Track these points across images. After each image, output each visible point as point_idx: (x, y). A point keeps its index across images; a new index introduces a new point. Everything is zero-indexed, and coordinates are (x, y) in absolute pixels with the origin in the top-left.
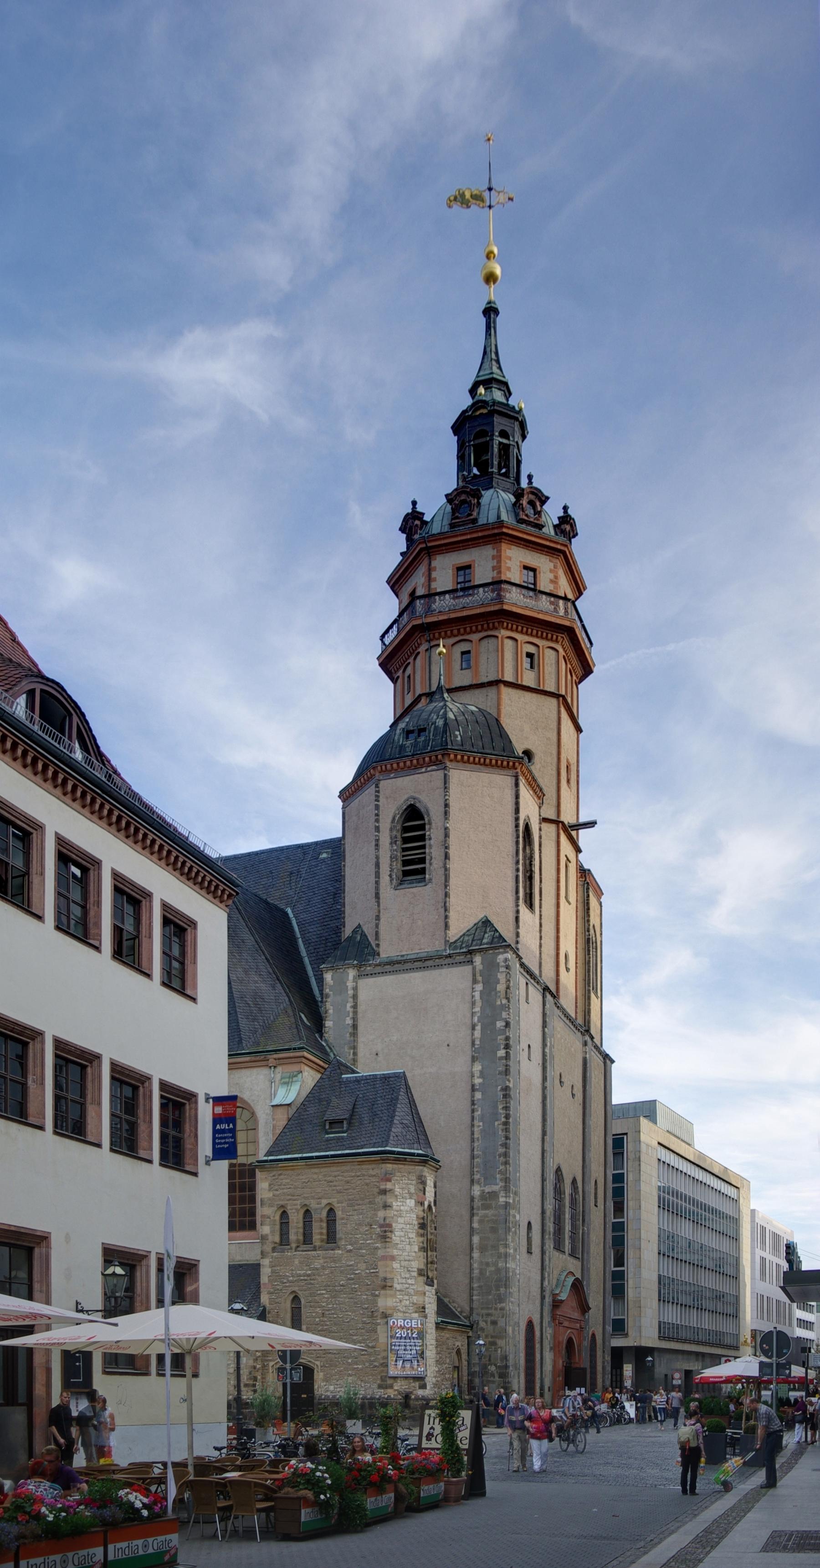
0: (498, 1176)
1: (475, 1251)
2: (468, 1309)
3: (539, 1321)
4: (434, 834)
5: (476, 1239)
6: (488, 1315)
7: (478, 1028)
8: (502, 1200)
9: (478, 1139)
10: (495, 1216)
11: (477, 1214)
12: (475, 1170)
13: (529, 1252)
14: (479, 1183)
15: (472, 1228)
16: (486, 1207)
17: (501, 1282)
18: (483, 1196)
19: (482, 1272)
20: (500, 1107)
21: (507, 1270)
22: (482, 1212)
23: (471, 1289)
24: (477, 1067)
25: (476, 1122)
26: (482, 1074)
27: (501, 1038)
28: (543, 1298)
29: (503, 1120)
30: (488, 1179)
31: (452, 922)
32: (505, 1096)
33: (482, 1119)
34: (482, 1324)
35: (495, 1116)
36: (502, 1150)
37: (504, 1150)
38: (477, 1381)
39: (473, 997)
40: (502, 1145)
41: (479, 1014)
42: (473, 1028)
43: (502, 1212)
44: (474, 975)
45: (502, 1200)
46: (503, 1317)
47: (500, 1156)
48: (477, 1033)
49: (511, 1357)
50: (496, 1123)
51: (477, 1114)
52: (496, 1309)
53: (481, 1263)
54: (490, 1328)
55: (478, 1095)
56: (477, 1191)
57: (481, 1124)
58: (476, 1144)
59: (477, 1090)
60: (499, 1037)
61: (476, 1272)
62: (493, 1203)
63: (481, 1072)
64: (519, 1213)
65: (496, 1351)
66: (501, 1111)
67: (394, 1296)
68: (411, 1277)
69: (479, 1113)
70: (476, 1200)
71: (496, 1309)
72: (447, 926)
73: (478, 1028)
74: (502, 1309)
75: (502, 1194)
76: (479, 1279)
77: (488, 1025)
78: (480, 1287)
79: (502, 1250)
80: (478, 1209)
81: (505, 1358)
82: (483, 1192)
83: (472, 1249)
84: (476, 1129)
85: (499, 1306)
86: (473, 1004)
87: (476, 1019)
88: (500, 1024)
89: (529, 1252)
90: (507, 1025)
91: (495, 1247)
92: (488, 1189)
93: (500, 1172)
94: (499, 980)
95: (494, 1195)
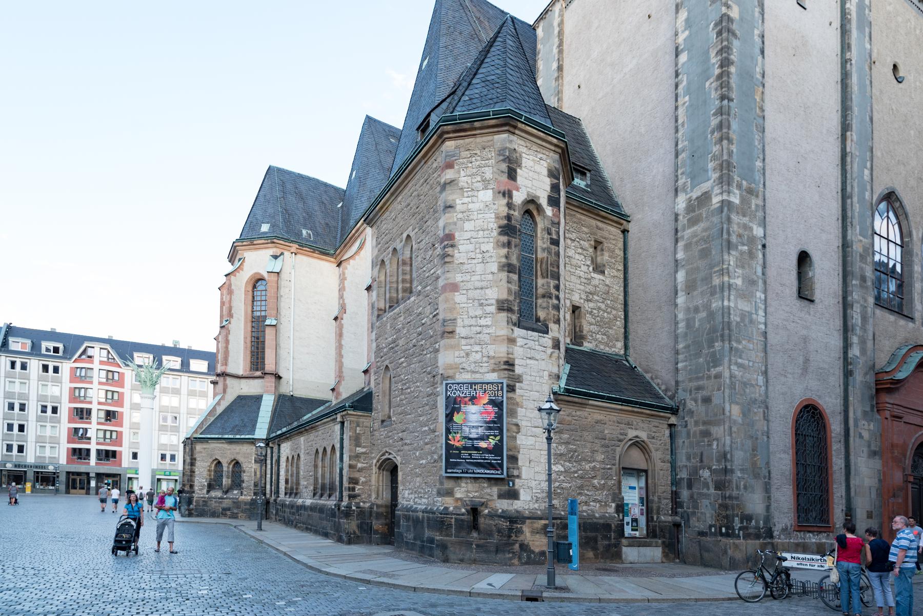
1: (680, 294)
2: (673, 383)
3: (839, 408)
6: (699, 388)
10: (705, 230)
11: (683, 237)
12: (680, 172)
13: (804, 294)
14: (684, 190)
15: (676, 261)
16: (693, 222)
18: (690, 208)
19: (689, 323)
21: (726, 311)
22: (688, 232)
23: (677, 353)
28: (847, 374)
34: (690, 404)
46: (719, 390)
49: (739, 458)
52: (709, 377)
53: (688, 310)
54: (701, 409)
56: (681, 203)
61: (682, 325)
62: (704, 212)
65: (710, 445)
67: (456, 347)
68: (486, 315)
70: (681, 218)
71: (709, 377)
74: (718, 376)
76: (686, 334)
78: (687, 347)
80: (684, 230)
81: (724, 456)
82: (690, 200)
83: (676, 293)
85: (713, 371)
89: (804, 294)
91: (708, 279)
92: (696, 194)
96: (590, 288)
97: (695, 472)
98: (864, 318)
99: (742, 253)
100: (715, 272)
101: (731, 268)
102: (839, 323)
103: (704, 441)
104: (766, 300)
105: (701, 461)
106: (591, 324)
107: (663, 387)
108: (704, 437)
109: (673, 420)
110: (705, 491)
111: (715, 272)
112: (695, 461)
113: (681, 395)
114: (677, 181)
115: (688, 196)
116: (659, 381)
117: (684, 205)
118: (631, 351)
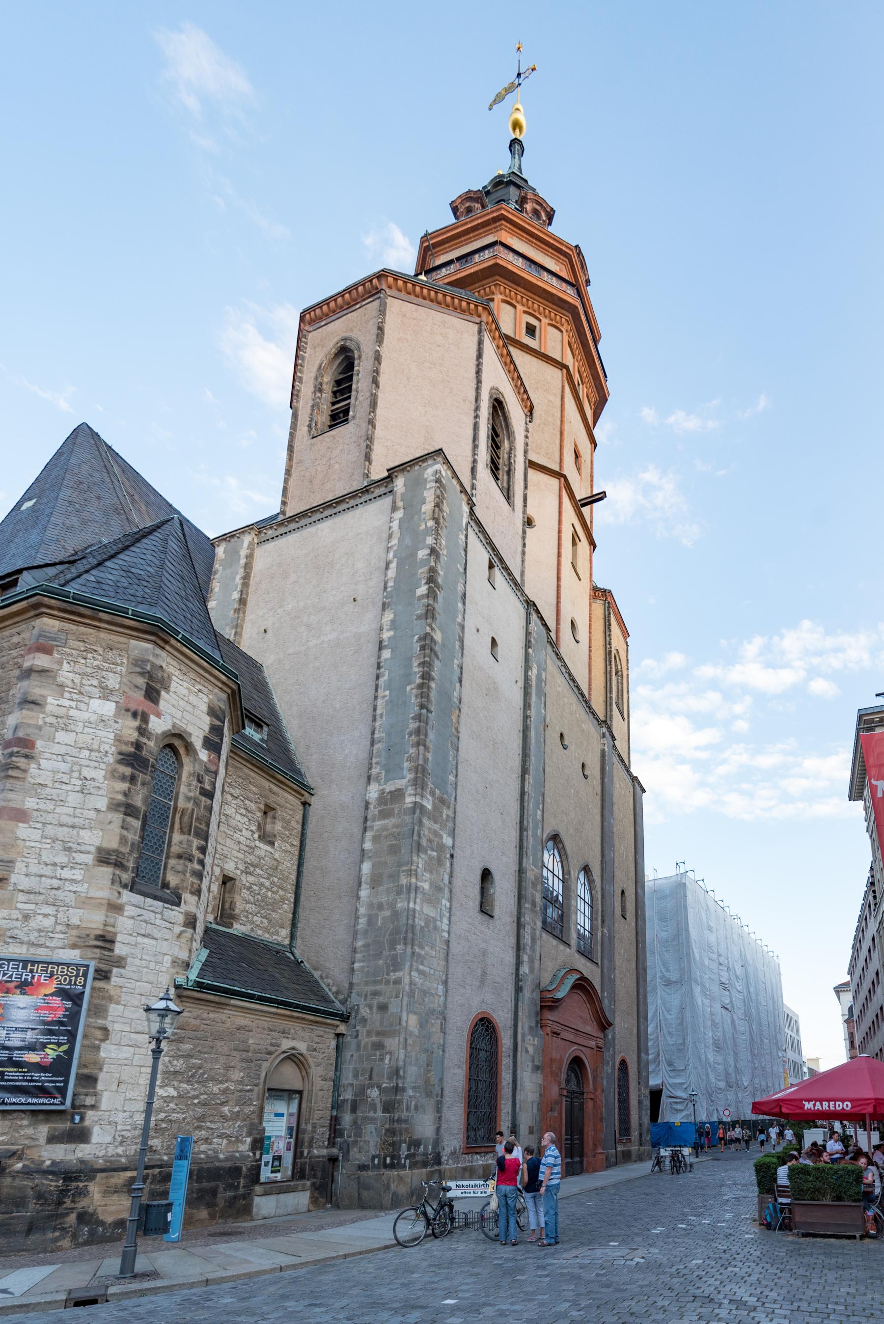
0: (406, 765)
4: (363, 368)
5: (366, 867)
7: (393, 566)
8: (409, 800)
9: (381, 716)
10: (397, 826)
12: (374, 761)
14: (377, 780)
17: (398, 936)
20: (415, 664)
22: (378, 824)
24: (389, 616)
25: (381, 693)
26: (394, 625)
27: (423, 572)
29: (419, 681)
30: (392, 771)
31: (374, 456)
32: (423, 648)
33: (388, 687)
35: (407, 678)
36: (413, 725)
37: (417, 724)
38: (347, 1119)
39: (390, 528)
40: (413, 718)
41: (395, 548)
42: (387, 568)
43: (408, 819)
44: (394, 502)
45: (409, 800)
47: (410, 734)
48: (392, 573)
50: (408, 688)
51: (382, 681)
54: (374, 1018)
55: (386, 654)
56: (373, 792)
57: (387, 693)
58: (377, 724)
59: (386, 647)
60: (420, 571)
62: (396, 808)
63: (393, 622)
64: (453, 834)
66: (416, 670)
69: (386, 678)
70: (371, 807)
72: (368, 458)
73: (393, 566)
75: (410, 790)
77: (406, 559)
79: (404, 881)
80: (374, 821)
82: (382, 792)
84: (380, 702)
86: (390, 536)
87: (391, 555)
88: (422, 554)
90: (434, 552)
92: (389, 788)
93: (410, 759)
94: (424, 499)
95: (398, 795)
96: (251, 858)
97: (361, 1091)
98: (533, 940)
99: (431, 858)
100: (403, 871)
101: (419, 871)
102: (512, 940)
103: (375, 1055)
104: (450, 908)
105: (371, 1078)
106: (248, 902)
107: (334, 989)
108: (376, 1049)
109: (342, 1028)
110: (371, 1114)
111: (403, 871)
112: (363, 1079)
113: (354, 999)
114: (370, 769)
115: (381, 787)
116: (330, 981)
117: (376, 795)
118: (298, 942)
